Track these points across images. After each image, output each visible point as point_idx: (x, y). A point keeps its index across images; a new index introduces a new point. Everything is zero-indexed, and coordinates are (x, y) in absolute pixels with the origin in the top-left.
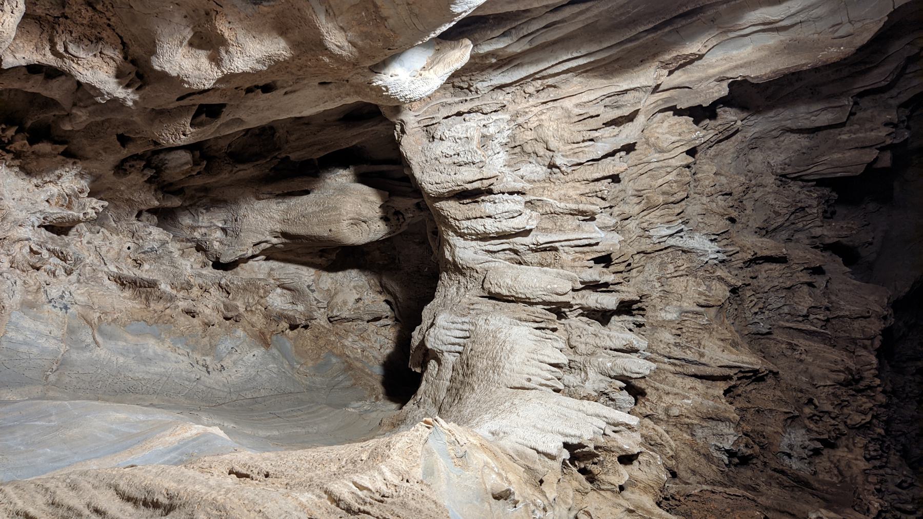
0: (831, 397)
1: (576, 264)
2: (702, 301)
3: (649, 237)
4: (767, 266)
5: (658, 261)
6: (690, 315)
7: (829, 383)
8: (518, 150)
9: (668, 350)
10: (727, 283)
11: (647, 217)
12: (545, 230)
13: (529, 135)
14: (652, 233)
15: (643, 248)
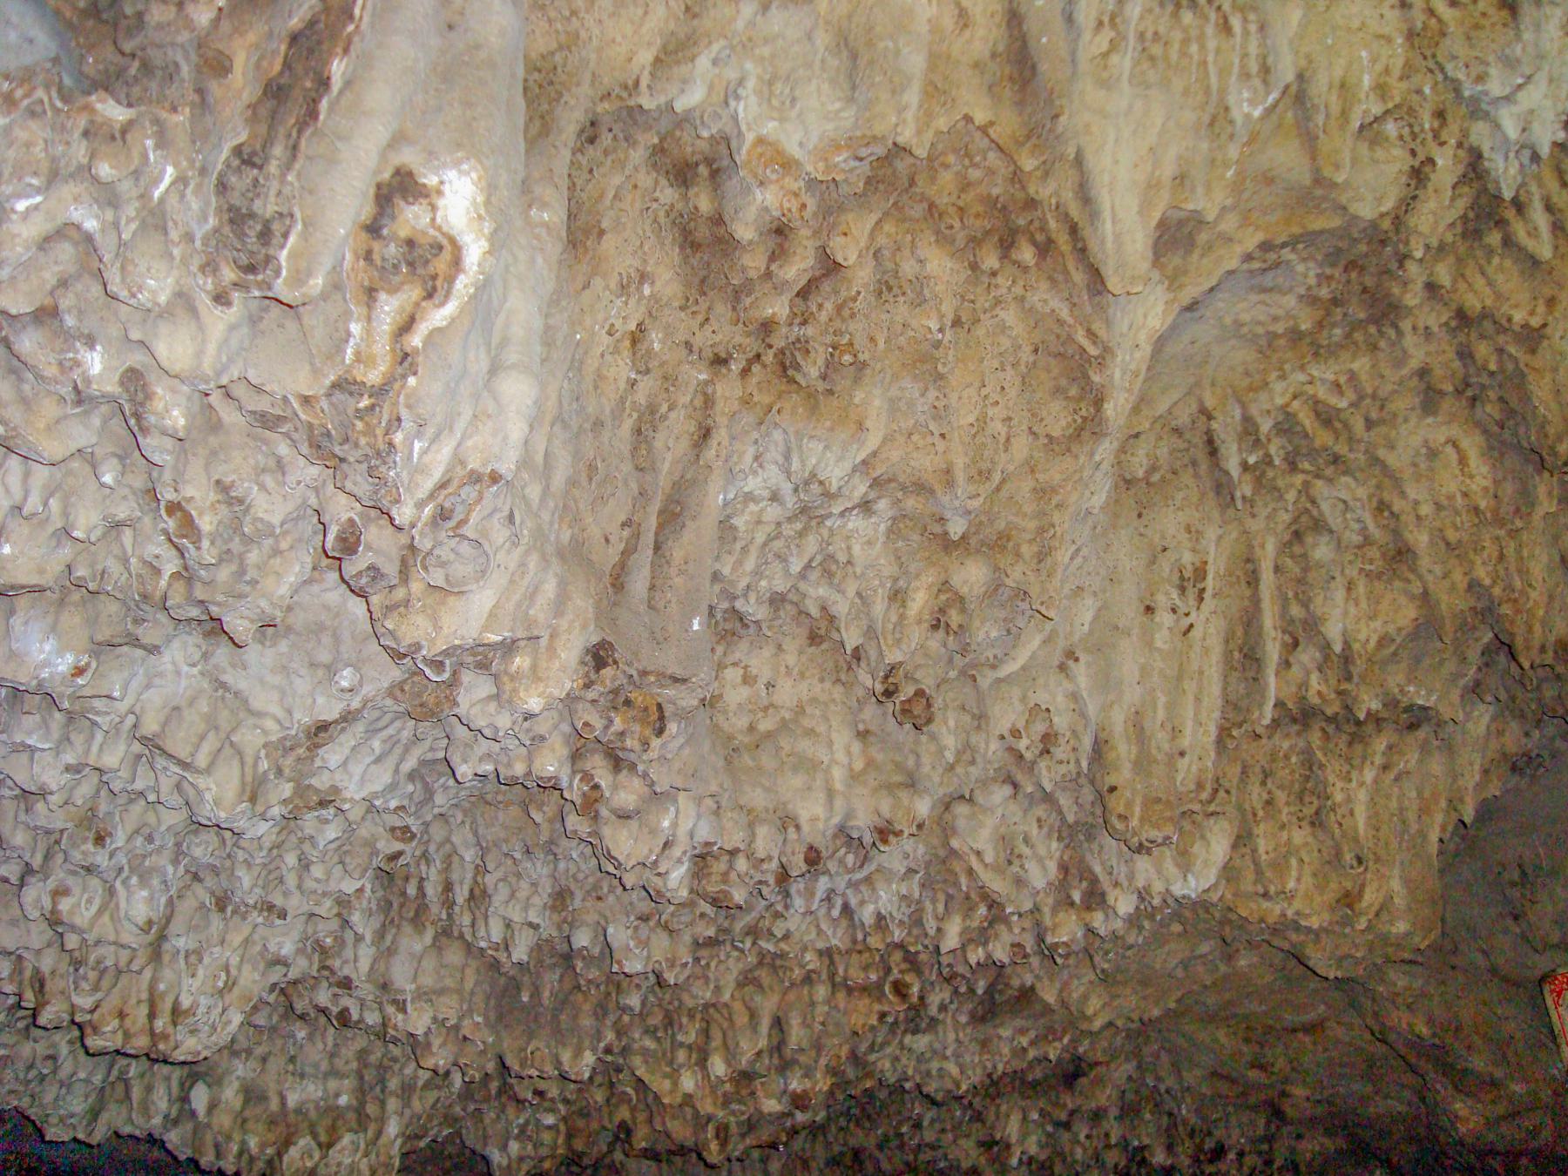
0: (1040, 727)
2: (1321, 88)
4: (1472, 444)
6: (1253, 48)
7: (1092, 709)
10: (1408, 203)
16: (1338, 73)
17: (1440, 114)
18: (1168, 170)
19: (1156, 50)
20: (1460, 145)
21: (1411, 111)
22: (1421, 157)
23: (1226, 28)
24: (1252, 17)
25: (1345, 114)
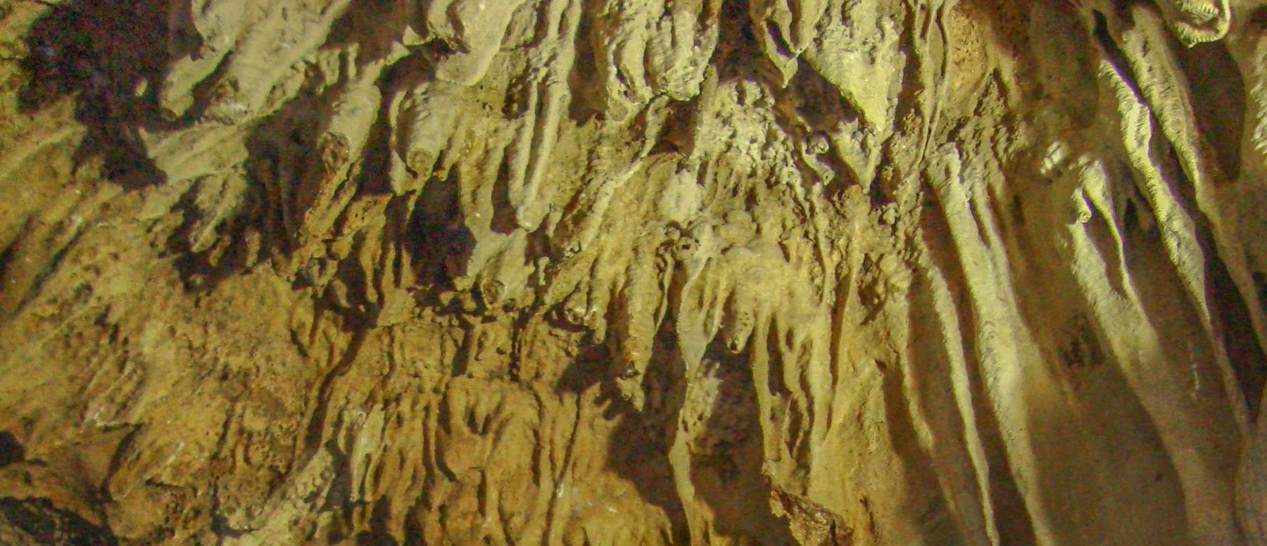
1: (462, 133)
2: (143, 443)
3: (369, 403)
5: (291, 403)
6: (128, 388)
8: (740, 200)
9: (86, 260)
11: (418, 423)
12: (559, 132)
13: (771, 232)
14: (377, 416)
15: (353, 373)
16: (160, 442)
17: (197, 512)
18: (25, 411)
19: (74, 342)
20: (194, 536)
21: (183, 497)
22: (169, 525)
23: (121, 366)
24: (140, 372)
25: (146, 468)
